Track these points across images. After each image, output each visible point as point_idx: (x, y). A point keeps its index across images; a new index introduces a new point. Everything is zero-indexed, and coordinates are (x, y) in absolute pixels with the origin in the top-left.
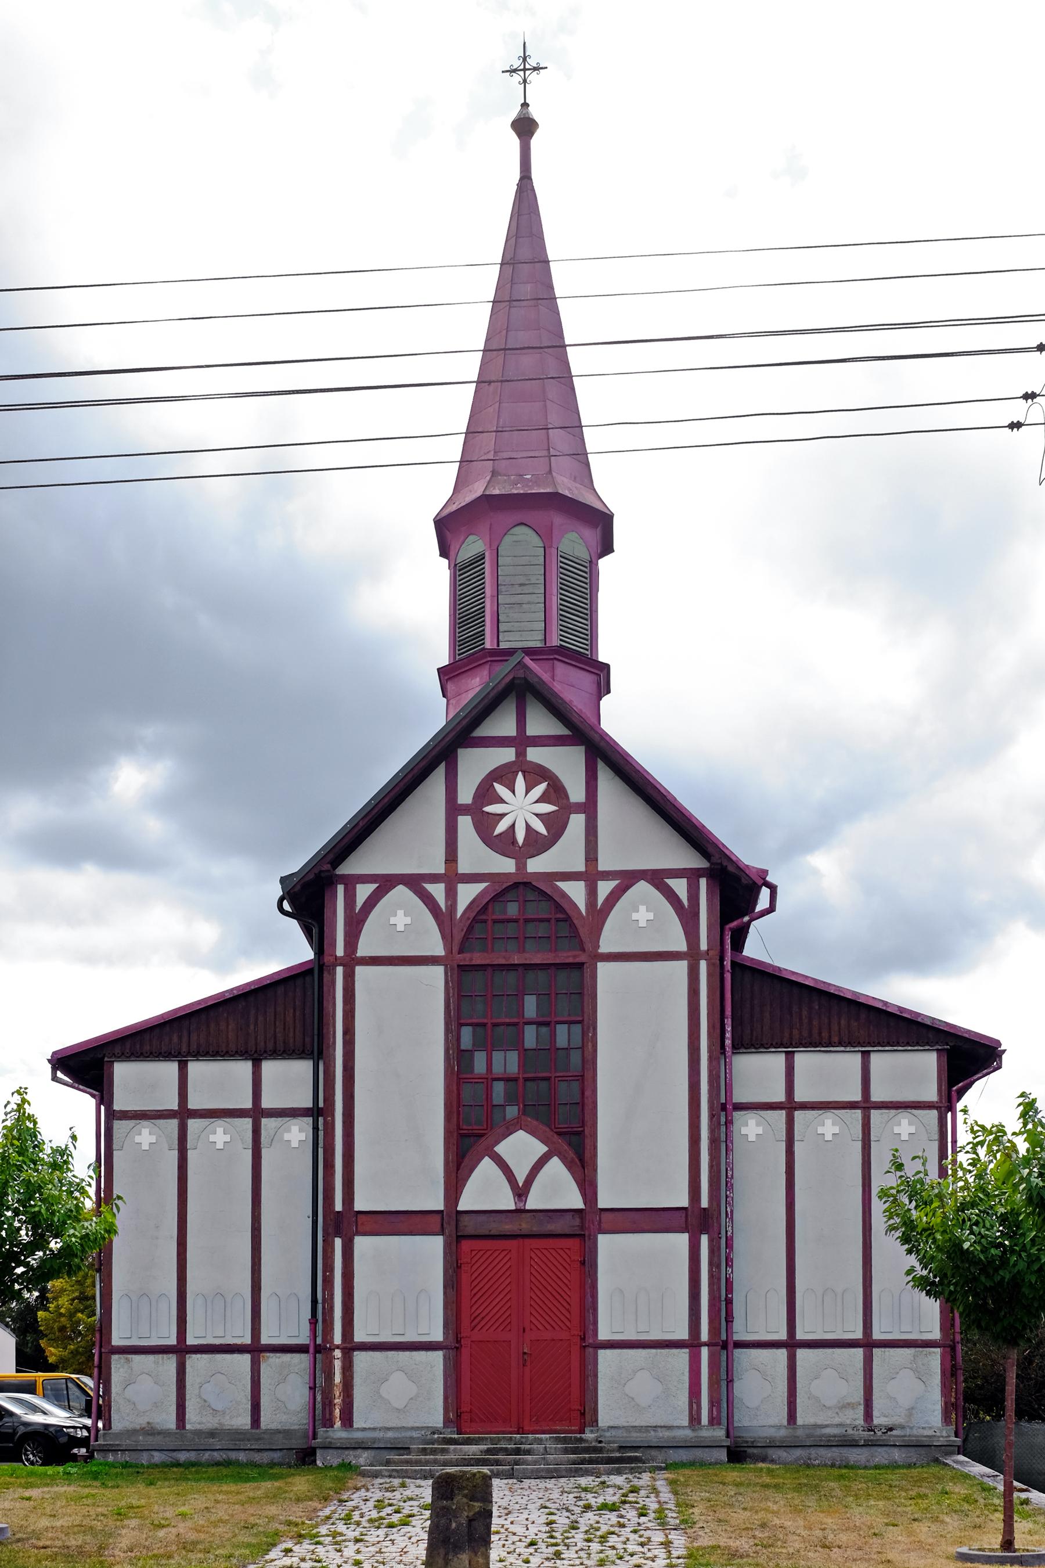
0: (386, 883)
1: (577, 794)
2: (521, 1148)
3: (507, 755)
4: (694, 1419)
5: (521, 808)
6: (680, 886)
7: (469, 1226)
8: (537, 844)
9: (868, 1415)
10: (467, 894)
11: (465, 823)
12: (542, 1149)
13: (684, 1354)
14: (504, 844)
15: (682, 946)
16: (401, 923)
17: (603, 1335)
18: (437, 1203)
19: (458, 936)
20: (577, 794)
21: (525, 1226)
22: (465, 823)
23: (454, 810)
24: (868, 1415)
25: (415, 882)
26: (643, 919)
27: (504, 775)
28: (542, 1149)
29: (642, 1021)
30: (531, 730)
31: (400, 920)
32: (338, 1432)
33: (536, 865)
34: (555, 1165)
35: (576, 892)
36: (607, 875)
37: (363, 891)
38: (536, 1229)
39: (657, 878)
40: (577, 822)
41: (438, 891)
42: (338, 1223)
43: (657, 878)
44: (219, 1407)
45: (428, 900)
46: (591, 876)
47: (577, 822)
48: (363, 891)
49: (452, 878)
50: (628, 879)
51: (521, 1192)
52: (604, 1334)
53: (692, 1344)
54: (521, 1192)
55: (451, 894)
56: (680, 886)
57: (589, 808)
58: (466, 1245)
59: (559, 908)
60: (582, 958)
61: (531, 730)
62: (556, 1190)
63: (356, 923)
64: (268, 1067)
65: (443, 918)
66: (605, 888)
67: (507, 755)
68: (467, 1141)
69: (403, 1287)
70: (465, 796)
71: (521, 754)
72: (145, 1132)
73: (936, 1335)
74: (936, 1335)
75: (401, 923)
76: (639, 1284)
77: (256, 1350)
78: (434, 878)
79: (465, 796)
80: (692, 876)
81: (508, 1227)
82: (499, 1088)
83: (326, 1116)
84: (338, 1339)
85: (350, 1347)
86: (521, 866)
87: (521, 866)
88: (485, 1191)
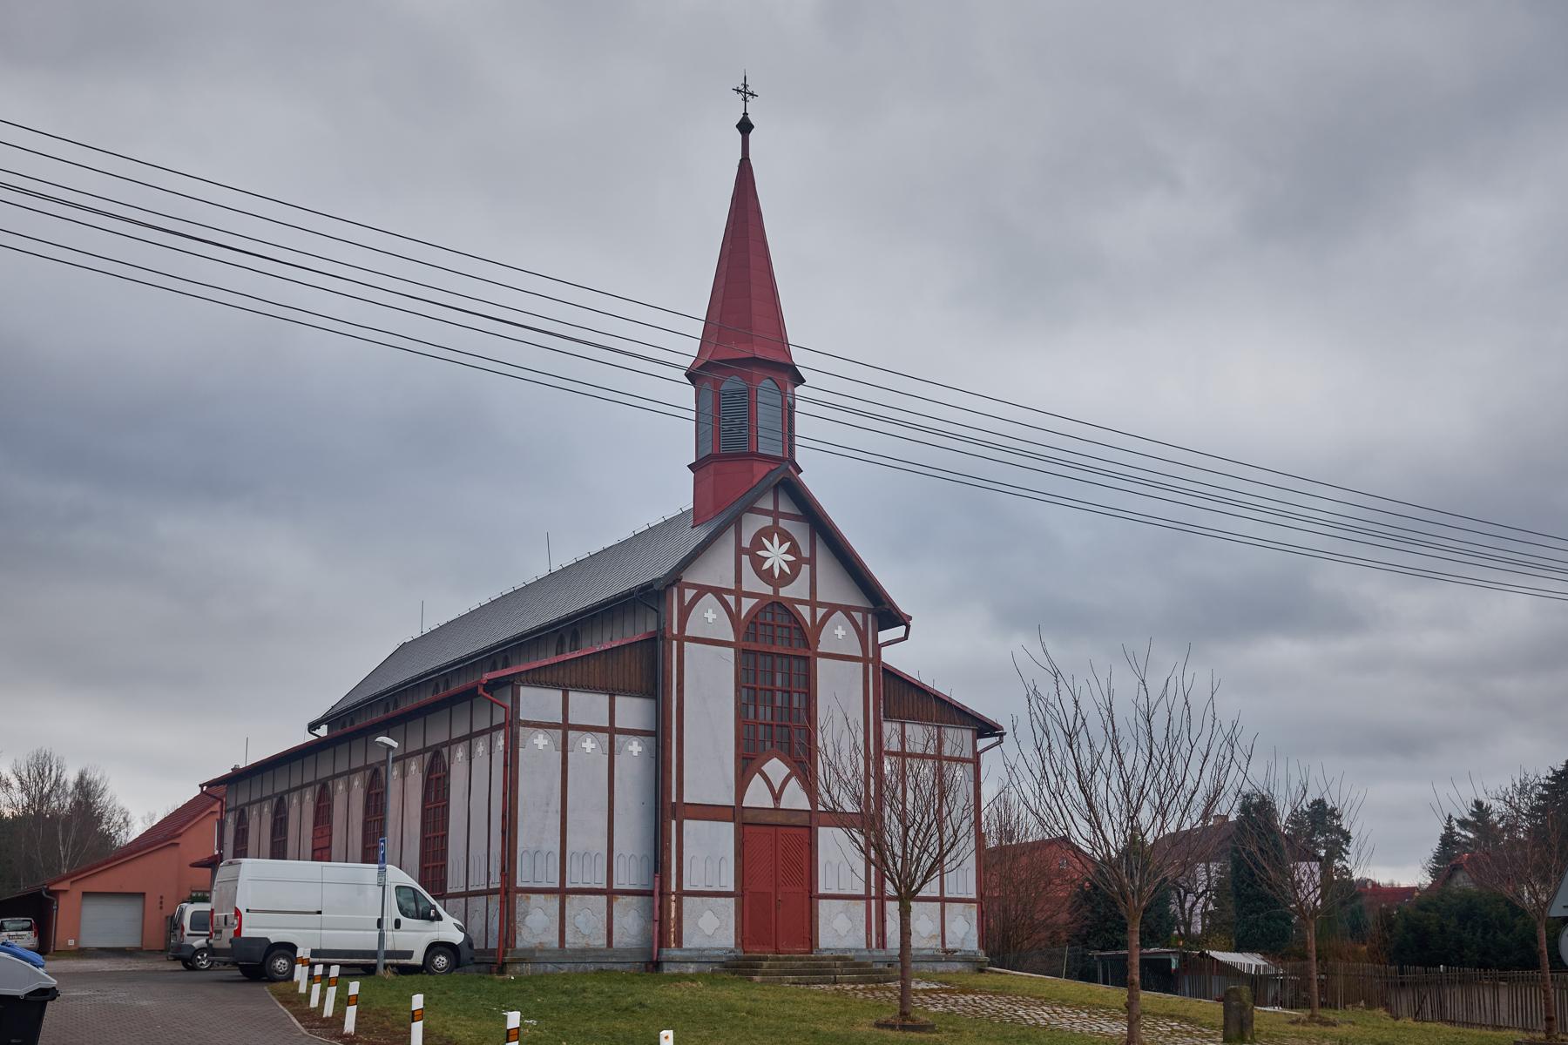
0: (702, 590)
1: (806, 553)
2: (776, 768)
3: (767, 521)
4: (869, 944)
5: (776, 555)
6: (858, 616)
7: (749, 817)
8: (786, 579)
9: (943, 943)
10: (747, 604)
11: (745, 559)
12: (787, 771)
13: (863, 904)
14: (766, 576)
15: (860, 654)
16: (709, 618)
17: (821, 891)
18: (728, 799)
19: (743, 630)
20: (806, 553)
21: (779, 819)
22: (745, 559)
23: (740, 551)
24: (943, 943)
25: (718, 592)
26: (838, 634)
27: (766, 533)
28: (787, 771)
29: (839, 698)
30: (781, 509)
31: (710, 616)
32: (672, 952)
33: (785, 592)
34: (793, 782)
35: (805, 611)
36: (822, 605)
37: (689, 594)
38: (784, 822)
39: (847, 610)
40: (805, 568)
41: (731, 599)
42: (667, 810)
43: (847, 610)
44: (587, 932)
45: (725, 604)
46: (813, 603)
47: (805, 568)
48: (689, 594)
49: (739, 594)
50: (832, 608)
51: (777, 798)
52: (821, 891)
53: (681, 894)
54: (777, 798)
55: (738, 603)
56: (858, 616)
57: (812, 561)
58: (747, 828)
59: (796, 621)
60: (809, 654)
61: (781, 509)
62: (795, 798)
63: (685, 613)
64: (619, 700)
65: (734, 617)
66: (820, 612)
67: (767, 521)
68: (747, 764)
69: (709, 855)
70: (746, 543)
71: (776, 522)
72: (541, 736)
73: (974, 896)
74: (974, 896)
75: (709, 618)
76: (839, 859)
77: (610, 893)
78: (729, 592)
79: (746, 543)
80: (865, 611)
81: (770, 820)
82: (761, 728)
83: (663, 740)
84: (674, 888)
85: (681, 894)
86: (776, 592)
87: (776, 592)
88: (757, 796)
